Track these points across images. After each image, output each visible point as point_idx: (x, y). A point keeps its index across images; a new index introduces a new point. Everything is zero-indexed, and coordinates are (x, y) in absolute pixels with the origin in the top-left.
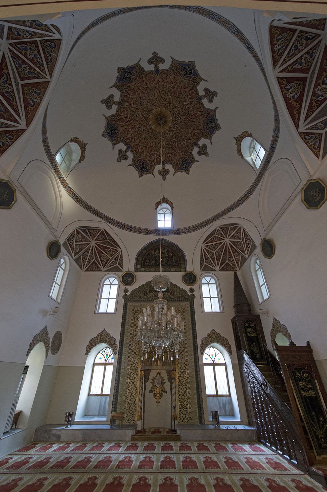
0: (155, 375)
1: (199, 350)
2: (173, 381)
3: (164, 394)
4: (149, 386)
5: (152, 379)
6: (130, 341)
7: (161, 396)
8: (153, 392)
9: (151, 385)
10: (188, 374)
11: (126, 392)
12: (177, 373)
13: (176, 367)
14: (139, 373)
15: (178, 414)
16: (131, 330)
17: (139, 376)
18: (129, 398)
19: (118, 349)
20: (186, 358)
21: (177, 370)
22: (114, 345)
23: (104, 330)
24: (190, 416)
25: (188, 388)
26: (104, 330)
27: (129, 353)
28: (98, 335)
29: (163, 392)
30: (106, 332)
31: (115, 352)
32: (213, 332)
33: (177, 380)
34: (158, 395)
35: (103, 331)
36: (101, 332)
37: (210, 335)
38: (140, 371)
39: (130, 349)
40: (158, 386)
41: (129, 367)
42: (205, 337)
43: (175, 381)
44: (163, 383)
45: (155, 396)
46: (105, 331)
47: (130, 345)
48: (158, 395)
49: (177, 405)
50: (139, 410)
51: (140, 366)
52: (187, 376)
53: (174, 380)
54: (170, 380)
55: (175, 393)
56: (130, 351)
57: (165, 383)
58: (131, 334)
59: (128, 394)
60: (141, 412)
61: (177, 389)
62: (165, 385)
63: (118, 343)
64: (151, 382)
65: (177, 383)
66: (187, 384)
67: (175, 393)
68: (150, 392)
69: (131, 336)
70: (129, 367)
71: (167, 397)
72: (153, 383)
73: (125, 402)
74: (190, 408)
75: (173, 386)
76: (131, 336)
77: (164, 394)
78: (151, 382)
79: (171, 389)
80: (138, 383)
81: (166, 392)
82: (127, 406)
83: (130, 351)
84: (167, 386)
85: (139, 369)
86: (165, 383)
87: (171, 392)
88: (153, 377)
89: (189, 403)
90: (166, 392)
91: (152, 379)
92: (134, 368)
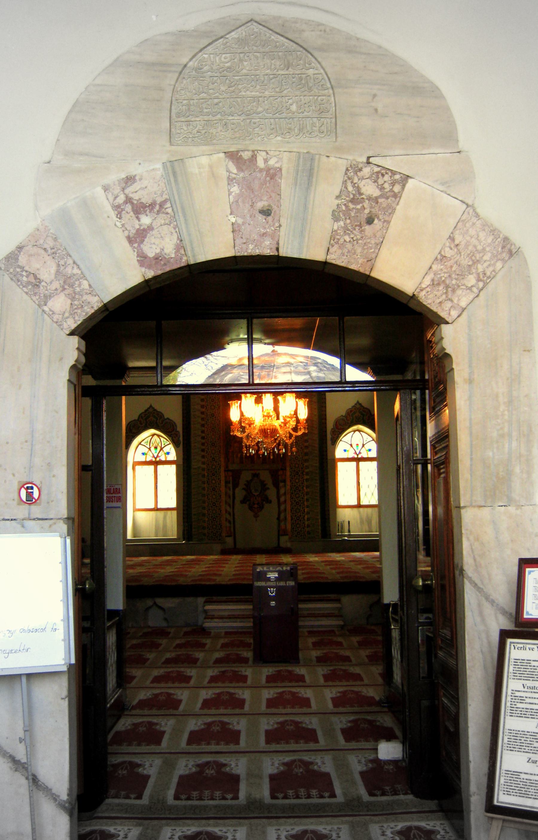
0: (249, 478)
1: (329, 436)
2: (281, 484)
3: (266, 505)
4: (240, 493)
5: (245, 485)
6: (203, 425)
7: (261, 508)
8: (248, 503)
9: (244, 493)
10: (307, 474)
11: (204, 502)
12: (288, 473)
13: (288, 464)
14: (223, 474)
15: (289, 527)
16: (202, 406)
17: (223, 478)
18: (209, 509)
19: (181, 439)
20: (305, 451)
21: (288, 469)
22: (173, 433)
23: (151, 406)
24: (307, 529)
25: (307, 493)
26: (151, 406)
27: (203, 444)
28: (140, 416)
29: (264, 502)
30: (155, 410)
31: (176, 444)
32: (358, 406)
33: (288, 483)
34: (256, 506)
35: (149, 408)
36: (146, 411)
37: (351, 411)
38: (225, 471)
39: (203, 438)
40: (256, 494)
41: (204, 466)
42: (342, 416)
43: (285, 486)
44: (264, 487)
45: (251, 508)
46: (153, 408)
47: (203, 432)
48: (256, 506)
49: (288, 517)
50: (228, 525)
51: (223, 463)
52: (306, 477)
53: (283, 484)
54: (276, 485)
55: (285, 501)
56: (203, 441)
57: (268, 488)
58: (202, 413)
59: (207, 504)
60: (230, 527)
61: (288, 497)
62: (268, 493)
63: (180, 428)
64: (244, 489)
65: (288, 487)
66: (305, 488)
67: (285, 501)
68: (243, 502)
69: (203, 416)
70: (204, 466)
71: (270, 511)
72: (248, 487)
73: (204, 515)
74: (308, 519)
75: (282, 491)
76: (203, 416)
77: (266, 505)
78: (244, 489)
79: (278, 497)
80: (223, 489)
81: (270, 502)
82: (207, 519)
83: (203, 441)
84: (272, 493)
85: (222, 469)
86: (268, 488)
87: (279, 507)
88: (247, 481)
89: (308, 513)
90: (270, 502)
91: (245, 485)
92: (214, 467)
